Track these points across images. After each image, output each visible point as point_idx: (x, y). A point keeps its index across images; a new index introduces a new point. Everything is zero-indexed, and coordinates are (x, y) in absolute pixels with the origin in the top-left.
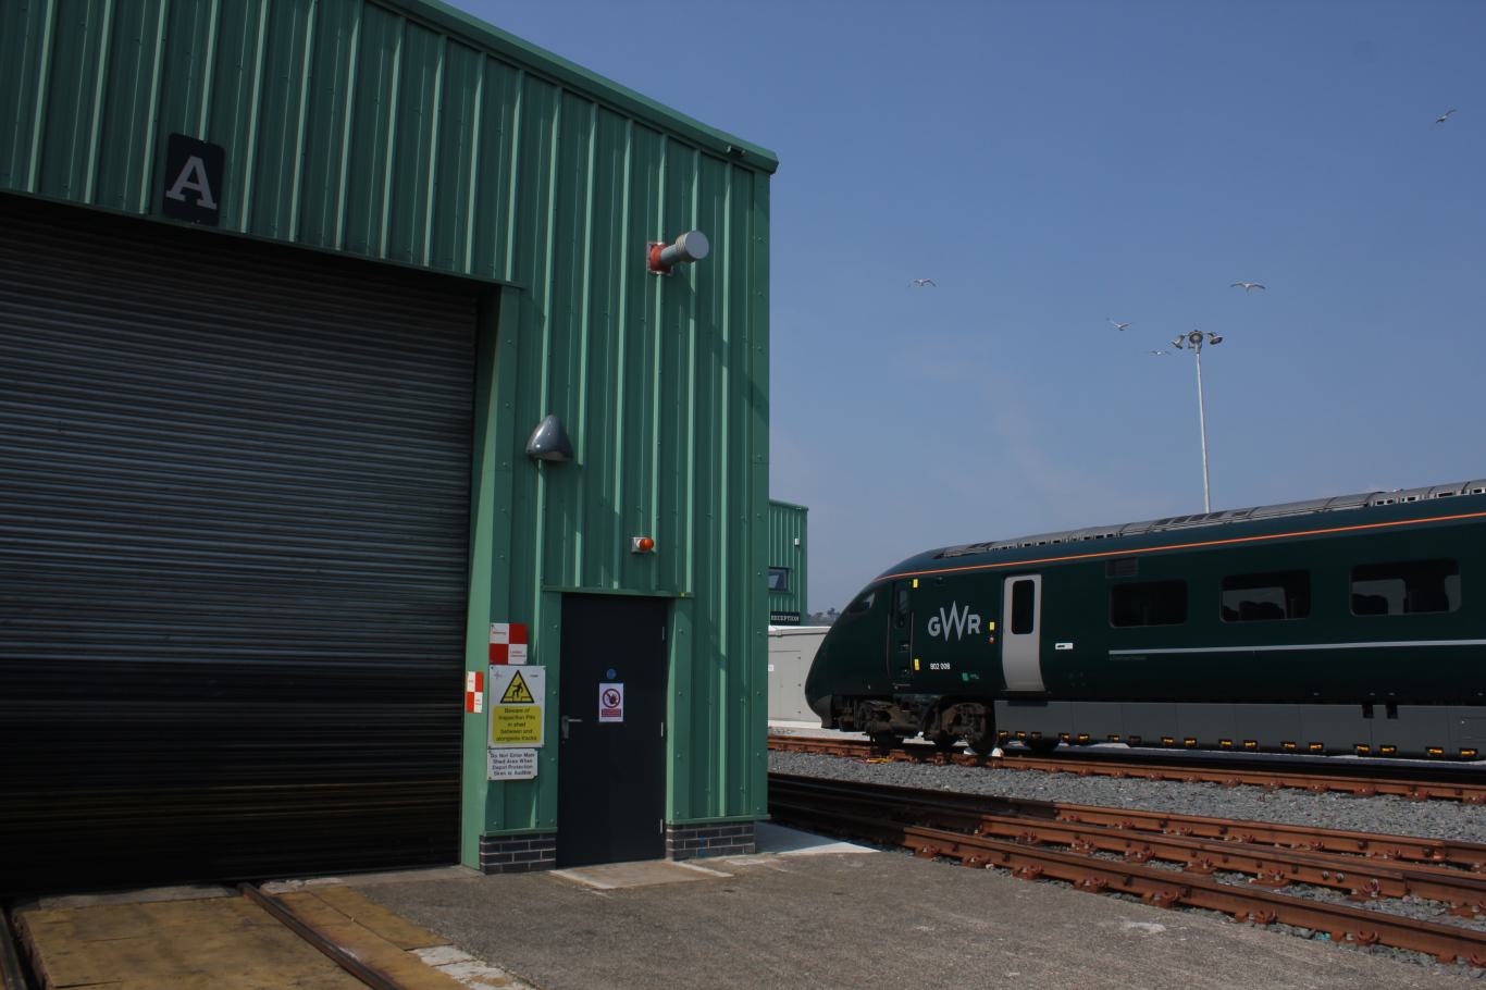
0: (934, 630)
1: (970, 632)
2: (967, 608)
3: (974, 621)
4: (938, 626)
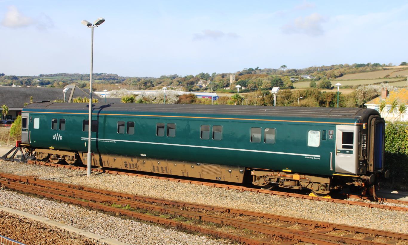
2: (60, 135)
4: (55, 137)
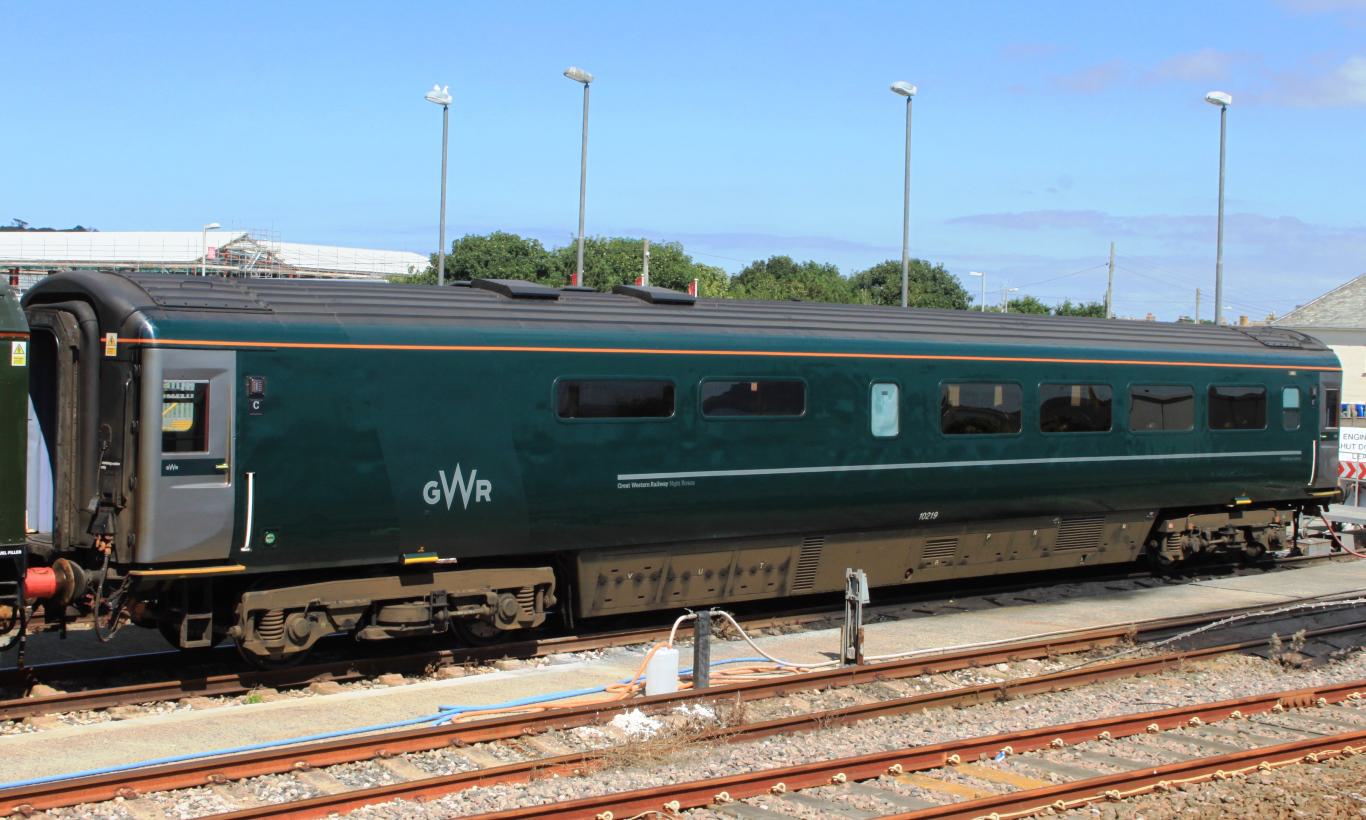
0: (432, 497)
1: (478, 499)
2: (474, 473)
3: (484, 488)
4: (437, 493)
